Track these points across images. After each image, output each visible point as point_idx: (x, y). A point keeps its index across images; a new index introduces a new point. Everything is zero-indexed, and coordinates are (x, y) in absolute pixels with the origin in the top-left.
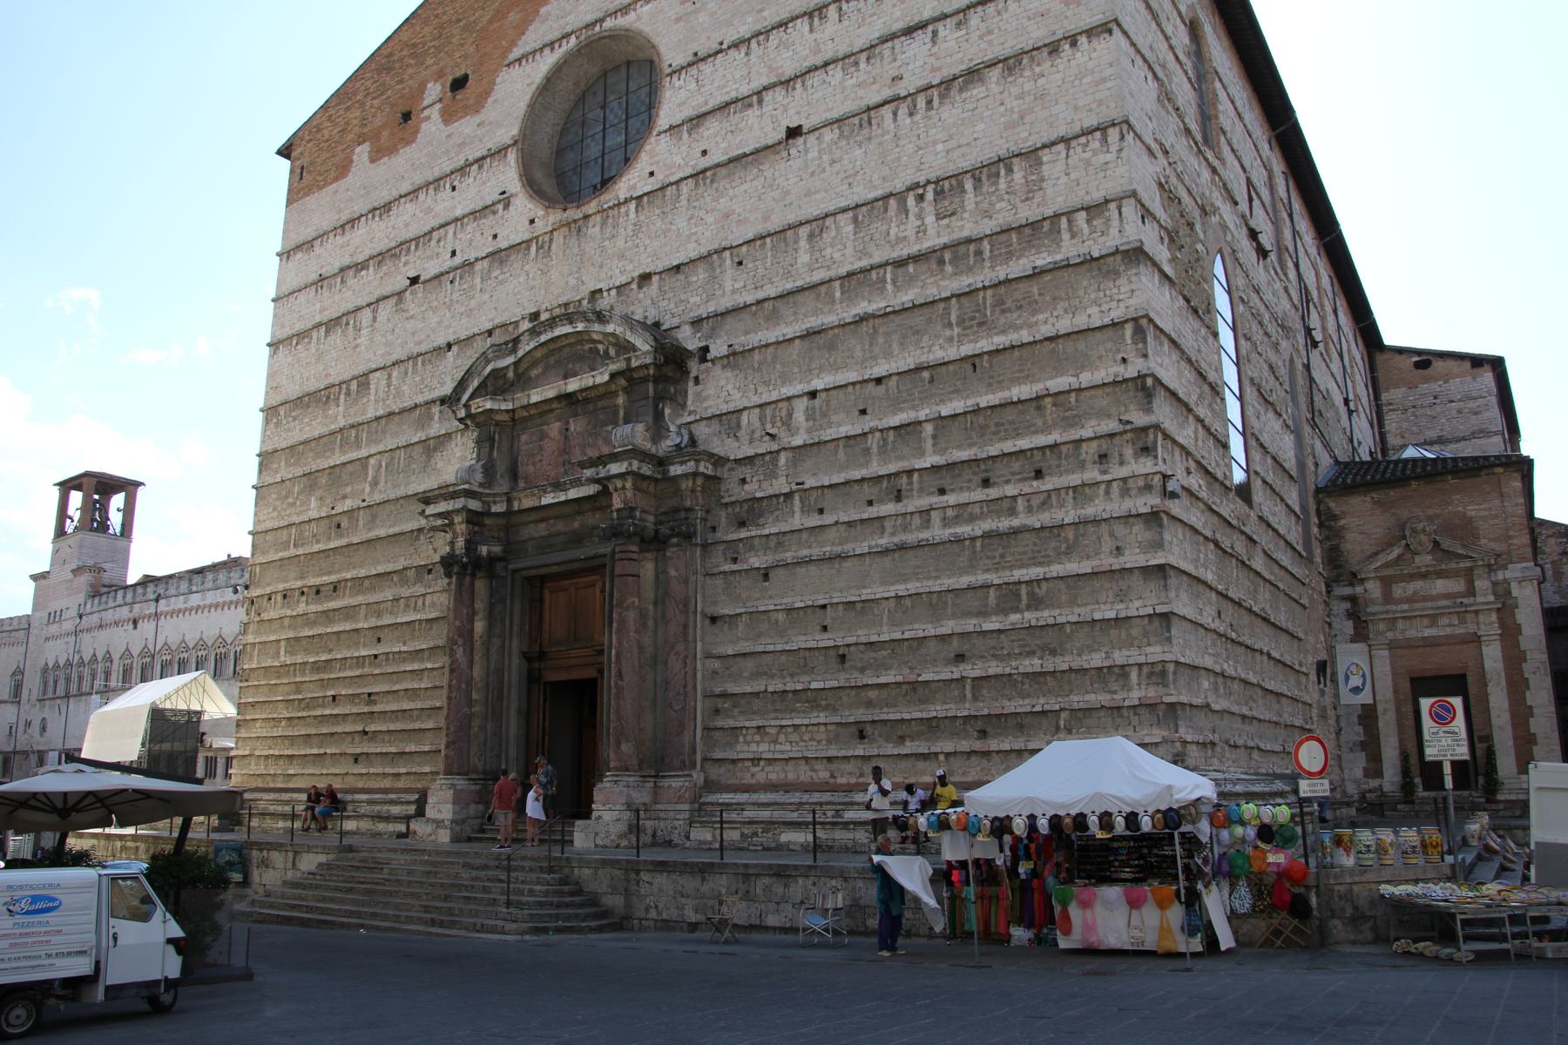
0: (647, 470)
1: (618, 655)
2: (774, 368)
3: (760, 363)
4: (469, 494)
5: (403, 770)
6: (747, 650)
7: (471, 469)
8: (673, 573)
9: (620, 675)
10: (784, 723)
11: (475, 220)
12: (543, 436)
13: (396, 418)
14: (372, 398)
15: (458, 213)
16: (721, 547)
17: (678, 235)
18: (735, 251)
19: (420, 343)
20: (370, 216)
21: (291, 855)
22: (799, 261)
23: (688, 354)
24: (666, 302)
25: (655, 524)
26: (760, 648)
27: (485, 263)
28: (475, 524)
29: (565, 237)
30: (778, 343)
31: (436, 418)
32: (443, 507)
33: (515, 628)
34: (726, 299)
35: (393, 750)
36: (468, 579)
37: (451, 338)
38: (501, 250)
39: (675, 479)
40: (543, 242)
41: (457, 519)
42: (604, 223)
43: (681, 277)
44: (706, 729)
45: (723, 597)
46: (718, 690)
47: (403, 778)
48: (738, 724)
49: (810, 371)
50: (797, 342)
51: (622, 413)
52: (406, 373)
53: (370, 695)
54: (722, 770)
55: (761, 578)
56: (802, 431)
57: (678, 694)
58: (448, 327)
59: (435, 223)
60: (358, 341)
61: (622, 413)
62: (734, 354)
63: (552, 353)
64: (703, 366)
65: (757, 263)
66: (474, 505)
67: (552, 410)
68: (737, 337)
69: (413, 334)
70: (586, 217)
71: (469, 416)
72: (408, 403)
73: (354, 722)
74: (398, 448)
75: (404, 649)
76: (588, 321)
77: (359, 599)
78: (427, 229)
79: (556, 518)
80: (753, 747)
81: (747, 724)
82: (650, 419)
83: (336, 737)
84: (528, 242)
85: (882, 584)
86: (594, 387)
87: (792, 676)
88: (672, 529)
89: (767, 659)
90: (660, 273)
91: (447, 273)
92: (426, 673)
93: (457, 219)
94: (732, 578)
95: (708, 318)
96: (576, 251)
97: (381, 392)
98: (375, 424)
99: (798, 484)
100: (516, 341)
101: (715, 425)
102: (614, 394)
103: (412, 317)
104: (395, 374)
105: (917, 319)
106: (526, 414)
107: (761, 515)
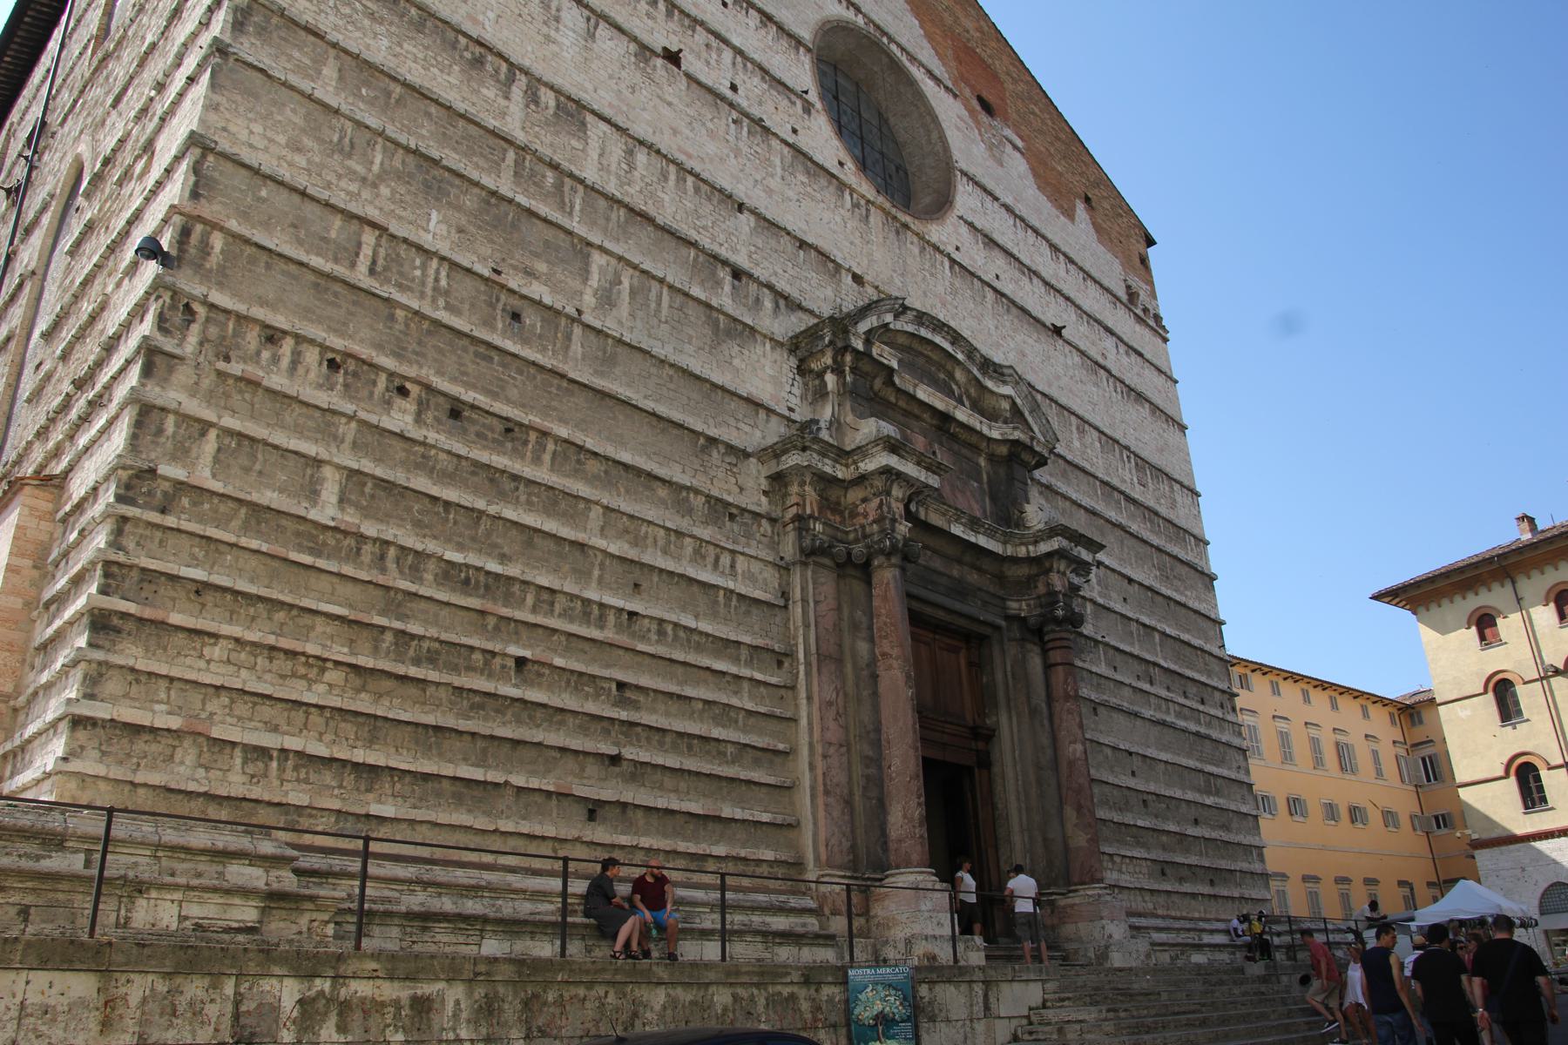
19: (690, 156)
21: (979, 989)
30: (1074, 503)
38: (811, 159)
51: (985, 477)
53: (621, 686)
67: (917, 418)
70: (906, 226)
73: (584, 730)
83: (524, 752)
85: (1157, 749)
105: (1143, 549)
106: (893, 399)
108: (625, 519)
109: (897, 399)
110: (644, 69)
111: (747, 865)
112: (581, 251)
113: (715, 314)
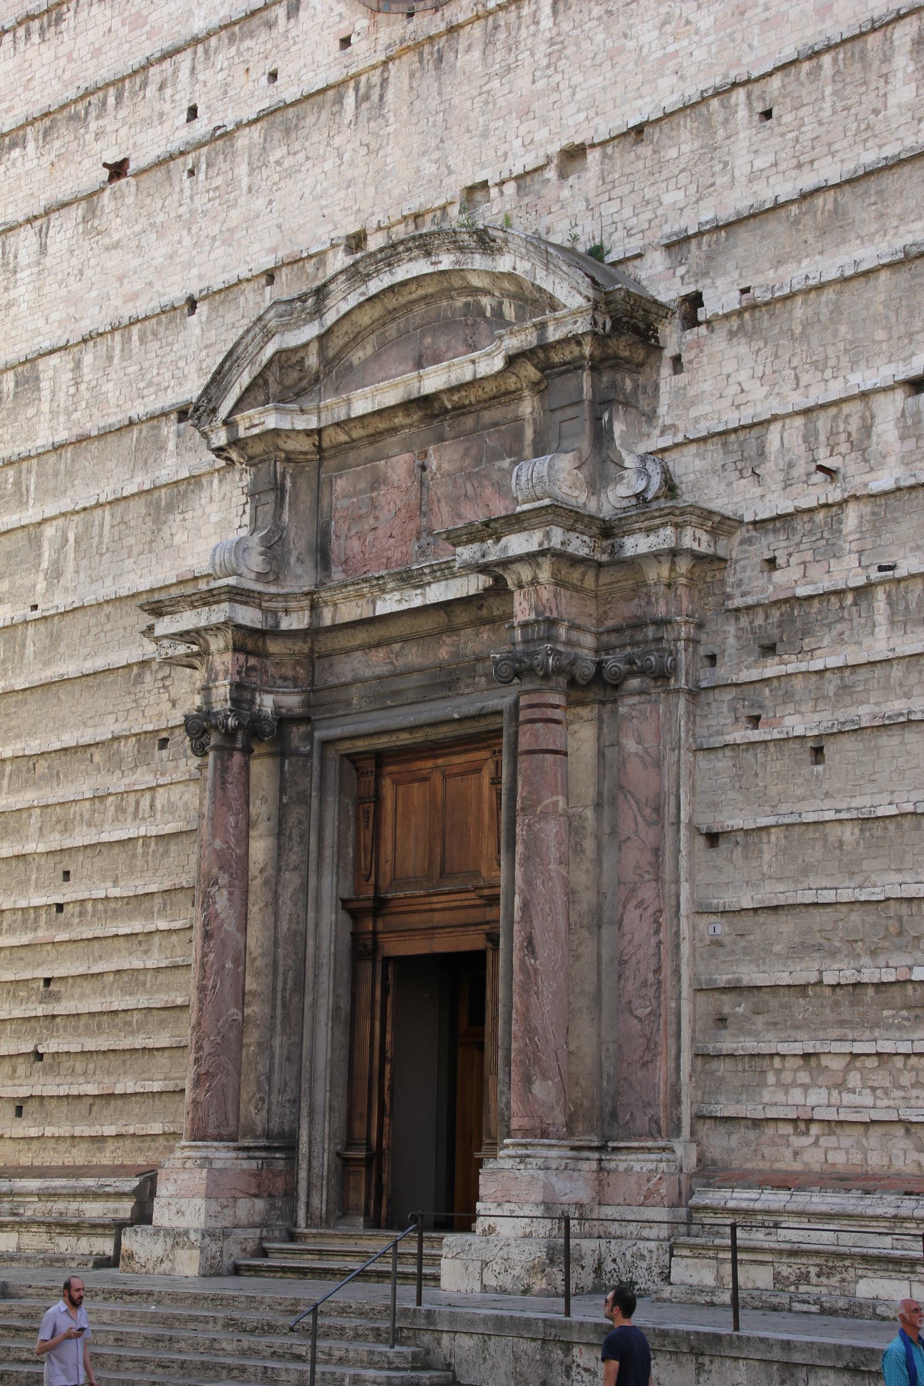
0: (579, 546)
1: (526, 905)
2: (835, 334)
3: (806, 325)
4: (237, 595)
5: (110, 1130)
6: (782, 900)
7: (240, 547)
8: (631, 745)
9: (530, 944)
10: (858, 1048)
11: (232, 39)
12: (377, 482)
13: (94, 447)
14: (45, 407)
15: (198, 26)
16: (728, 695)
17: (641, 60)
18: (756, 89)
19: (134, 297)
20: (21, 32)
22: (892, 101)
23: (663, 310)
24: (614, 206)
25: (597, 651)
26: (809, 897)
27: (256, 132)
28: (248, 653)
29: (412, 75)
30: (845, 280)
31: (171, 446)
32: (188, 620)
33: (328, 852)
34: (737, 192)
35: (91, 1089)
36: (237, 758)
37: (194, 289)
38: (287, 106)
39: (634, 563)
40: (369, 87)
41: (216, 643)
42: (489, 41)
43: (645, 150)
44: (702, 1056)
45: (731, 795)
46: (723, 979)
47: (110, 1145)
48: (765, 1049)
49: (910, 335)
50: (884, 275)
51: (529, 433)
52: (110, 358)
53: (48, 981)
54: (734, 1140)
55: (807, 757)
56: (892, 460)
57: (645, 984)
58: (189, 265)
59: (153, 48)
60: (13, 294)
61: (529, 433)
62: (754, 307)
63: (391, 314)
64: (691, 335)
65: (803, 112)
66: (248, 616)
67: (394, 430)
68: (759, 271)
69: (120, 279)
70: (453, 29)
71: (235, 442)
72: (115, 418)
74: (99, 505)
75: (115, 892)
76: (461, 249)
77: (28, 797)
78: (136, 61)
79: (405, 640)
80: (796, 1096)
81: (783, 1048)
82: (585, 444)
84: (341, 85)
86: (475, 382)
87: (873, 953)
88: (630, 661)
89: (821, 918)
90: (603, 144)
91: (182, 153)
92: (156, 939)
93: (196, 41)
94: (749, 756)
95: (700, 234)
96: (433, 103)
97: (61, 397)
98: (52, 458)
99: (881, 569)
100: (321, 293)
101: (714, 453)
102: (511, 396)
103: (116, 245)
104: (88, 359)
106: (343, 438)
107: (806, 632)
108: (58, 808)
109: (348, 433)
110: (92, 226)
111: (143, 1141)
112: (36, 537)
113: (156, 494)
